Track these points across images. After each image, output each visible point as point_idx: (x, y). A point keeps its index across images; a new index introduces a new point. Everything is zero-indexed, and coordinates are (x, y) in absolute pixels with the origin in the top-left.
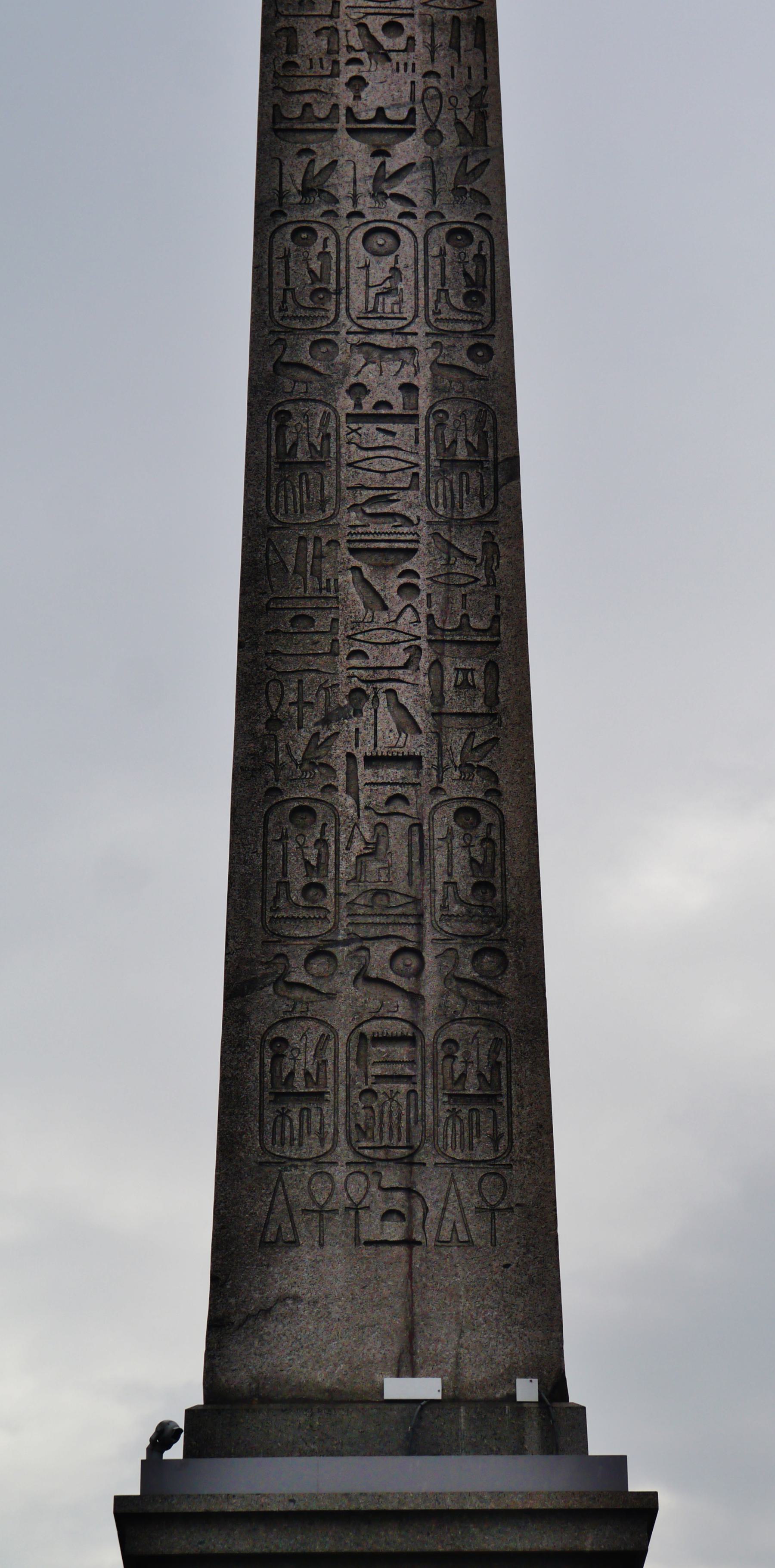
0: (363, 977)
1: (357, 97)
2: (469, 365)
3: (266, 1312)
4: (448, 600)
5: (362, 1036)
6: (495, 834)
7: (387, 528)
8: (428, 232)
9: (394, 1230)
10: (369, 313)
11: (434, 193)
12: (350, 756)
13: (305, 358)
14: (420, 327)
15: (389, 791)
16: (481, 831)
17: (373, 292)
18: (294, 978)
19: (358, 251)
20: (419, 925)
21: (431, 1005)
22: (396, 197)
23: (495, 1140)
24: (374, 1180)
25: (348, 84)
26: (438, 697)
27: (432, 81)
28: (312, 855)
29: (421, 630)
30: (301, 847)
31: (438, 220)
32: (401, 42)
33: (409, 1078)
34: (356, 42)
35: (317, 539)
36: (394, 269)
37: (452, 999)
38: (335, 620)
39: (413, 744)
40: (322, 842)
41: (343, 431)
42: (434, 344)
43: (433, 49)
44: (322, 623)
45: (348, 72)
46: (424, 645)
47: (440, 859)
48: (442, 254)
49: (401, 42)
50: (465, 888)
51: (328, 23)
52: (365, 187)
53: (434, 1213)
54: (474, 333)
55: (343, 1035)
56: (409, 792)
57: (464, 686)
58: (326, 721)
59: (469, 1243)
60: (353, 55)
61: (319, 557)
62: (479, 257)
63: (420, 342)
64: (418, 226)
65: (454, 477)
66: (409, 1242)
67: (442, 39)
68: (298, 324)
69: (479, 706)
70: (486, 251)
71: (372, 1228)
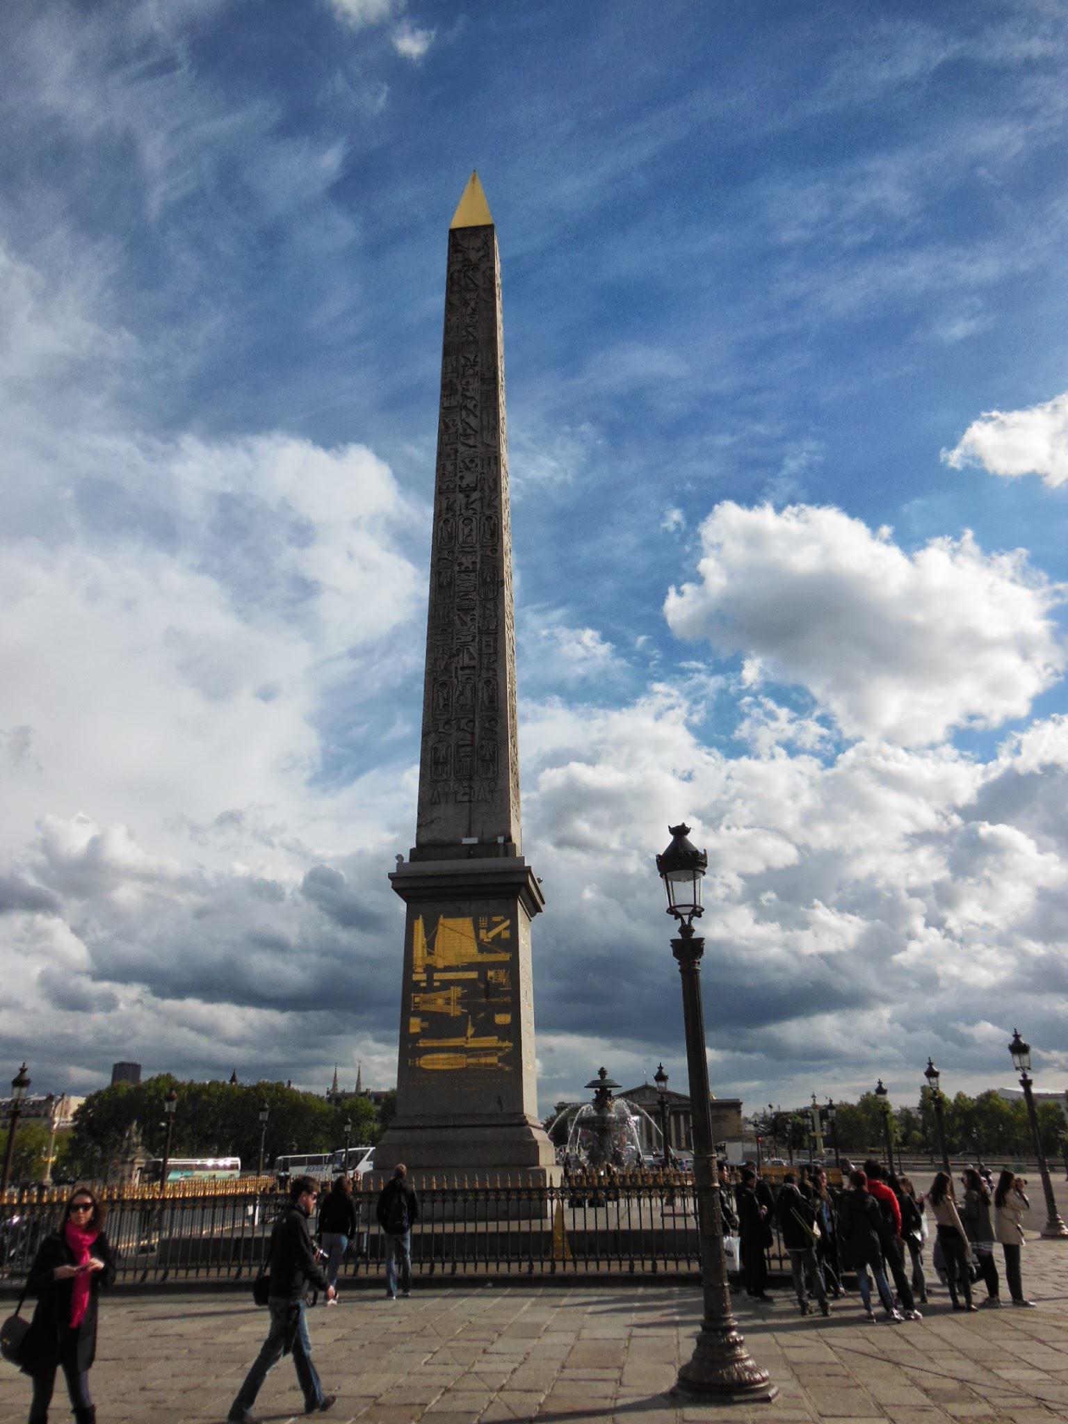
0: (459, 729)
2: (491, 554)
3: (432, 822)
8: (480, 519)
9: (466, 798)
10: (464, 542)
11: (482, 506)
12: (456, 667)
13: (446, 556)
14: (478, 545)
15: (466, 677)
16: (491, 687)
19: (461, 525)
20: (474, 714)
21: (477, 737)
23: (494, 773)
26: (480, 649)
28: (445, 695)
29: (476, 631)
30: (443, 694)
34: (461, 465)
36: (471, 530)
39: (473, 663)
40: (448, 692)
43: (483, 466)
44: (449, 631)
45: (459, 475)
47: (480, 694)
48: (484, 524)
52: (463, 506)
53: (476, 794)
54: (493, 546)
55: (453, 745)
57: (488, 646)
59: (486, 801)
61: (449, 612)
63: (477, 549)
64: (478, 516)
66: (470, 801)
67: (486, 462)
69: (492, 651)
71: (460, 798)
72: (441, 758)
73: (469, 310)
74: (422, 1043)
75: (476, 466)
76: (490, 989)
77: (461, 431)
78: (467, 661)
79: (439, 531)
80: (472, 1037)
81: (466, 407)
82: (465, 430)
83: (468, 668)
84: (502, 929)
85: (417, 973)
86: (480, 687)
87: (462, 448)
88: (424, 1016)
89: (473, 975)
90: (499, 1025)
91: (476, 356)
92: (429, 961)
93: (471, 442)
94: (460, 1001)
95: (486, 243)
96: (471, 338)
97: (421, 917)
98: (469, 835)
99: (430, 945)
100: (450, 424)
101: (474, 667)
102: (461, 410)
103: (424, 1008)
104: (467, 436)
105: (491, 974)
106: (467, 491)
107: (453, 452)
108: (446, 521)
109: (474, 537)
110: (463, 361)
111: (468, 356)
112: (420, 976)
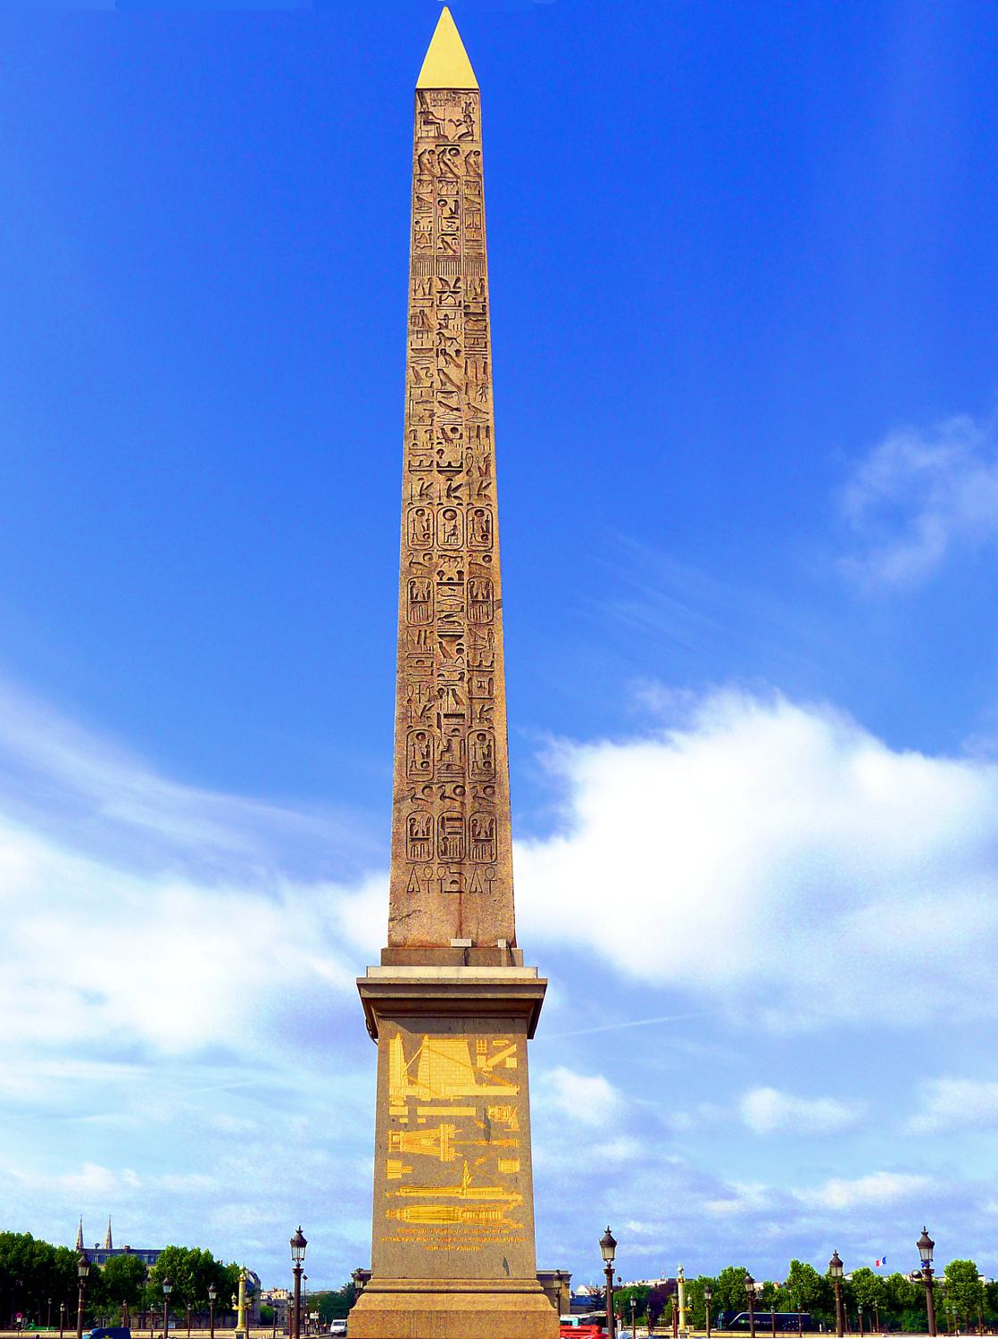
1: (441, 458)
2: (483, 564)
4: (475, 654)
5: (443, 818)
6: (492, 744)
7: (452, 627)
8: (468, 510)
9: (455, 887)
12: (438, 714)
13: (421, 561)
14: (465, 548)
15: (453, 727)
17: (447, 535)
18: (418, 796)
21: (468, 807)
22: (455, 497)
24: (447, 870)
25: (437, 453)
26: (470, 692)
27: (469, 451)
31: (470, 506)
32: (458, 435)
33: (460, 833)
35: (426, 631)
36: (455, 526)
37: (476, 804)
38: (433, 662)
39: (462, 710)
40: (428, 746)
41: (435, 589)
42: (470, 555)
45: (439, 447)
46: (466, 672)
47: (472, 753)
48: (473, 520)
49: (458, 435)
50: (480, 764)
51: (430, 428)
53: (469, 881)
56: (460, 728)
60: (439, 441)
62: (487, 521)
64: (464, 509)
65: (477, 607)
66: (460, 892)
67: (474, 434)
68: (417, 547)
70: (490, 519)
72: (420, 831)
73: (447, 213)
74: (402, 1193)
75: (461, 438)
77: (437, 385)
79: (411, 525)
80: (469, 1187)
81: (444, 353)
82: (443, 384)
85: (393, 1106)
86: (472, 743)
87: (440, 411)
89: (471, 1112)
90: (501, 1173)
91: (458, 280)
92: (411, 1091)
93: (453, 402)
96: (451, 253)
97: (398, 1035)
98: (460, 933)
99: (412, 1072)
100: (422, 373)
102: (437, 356)
103: (403, 1148)
106: (450, 471)
107: (428, 413)
109: (460, 537)
110: (438, 285)
111: (444, 278)
112: (398, 1110)
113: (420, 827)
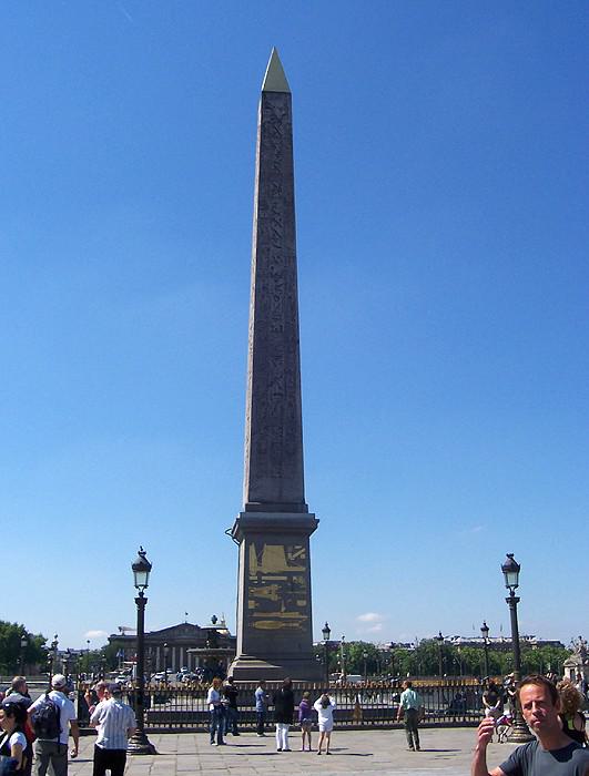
34: (271, 259)
58: (268, 386)
74: (255, 615)
76: (294, 586)
77: (271, 235)
78: (277, 391)
83: (279, 394)
84: (300, 553)
87: (272, 248)
88: (257, 600)
89: (285, 578)
94: (278, 592)
95: (285, 105)
99: (259, 560)
101: (281, 395)
104: (276, 240)
105: (295, 578)
108: (263, 296)
113: (263, 447)
